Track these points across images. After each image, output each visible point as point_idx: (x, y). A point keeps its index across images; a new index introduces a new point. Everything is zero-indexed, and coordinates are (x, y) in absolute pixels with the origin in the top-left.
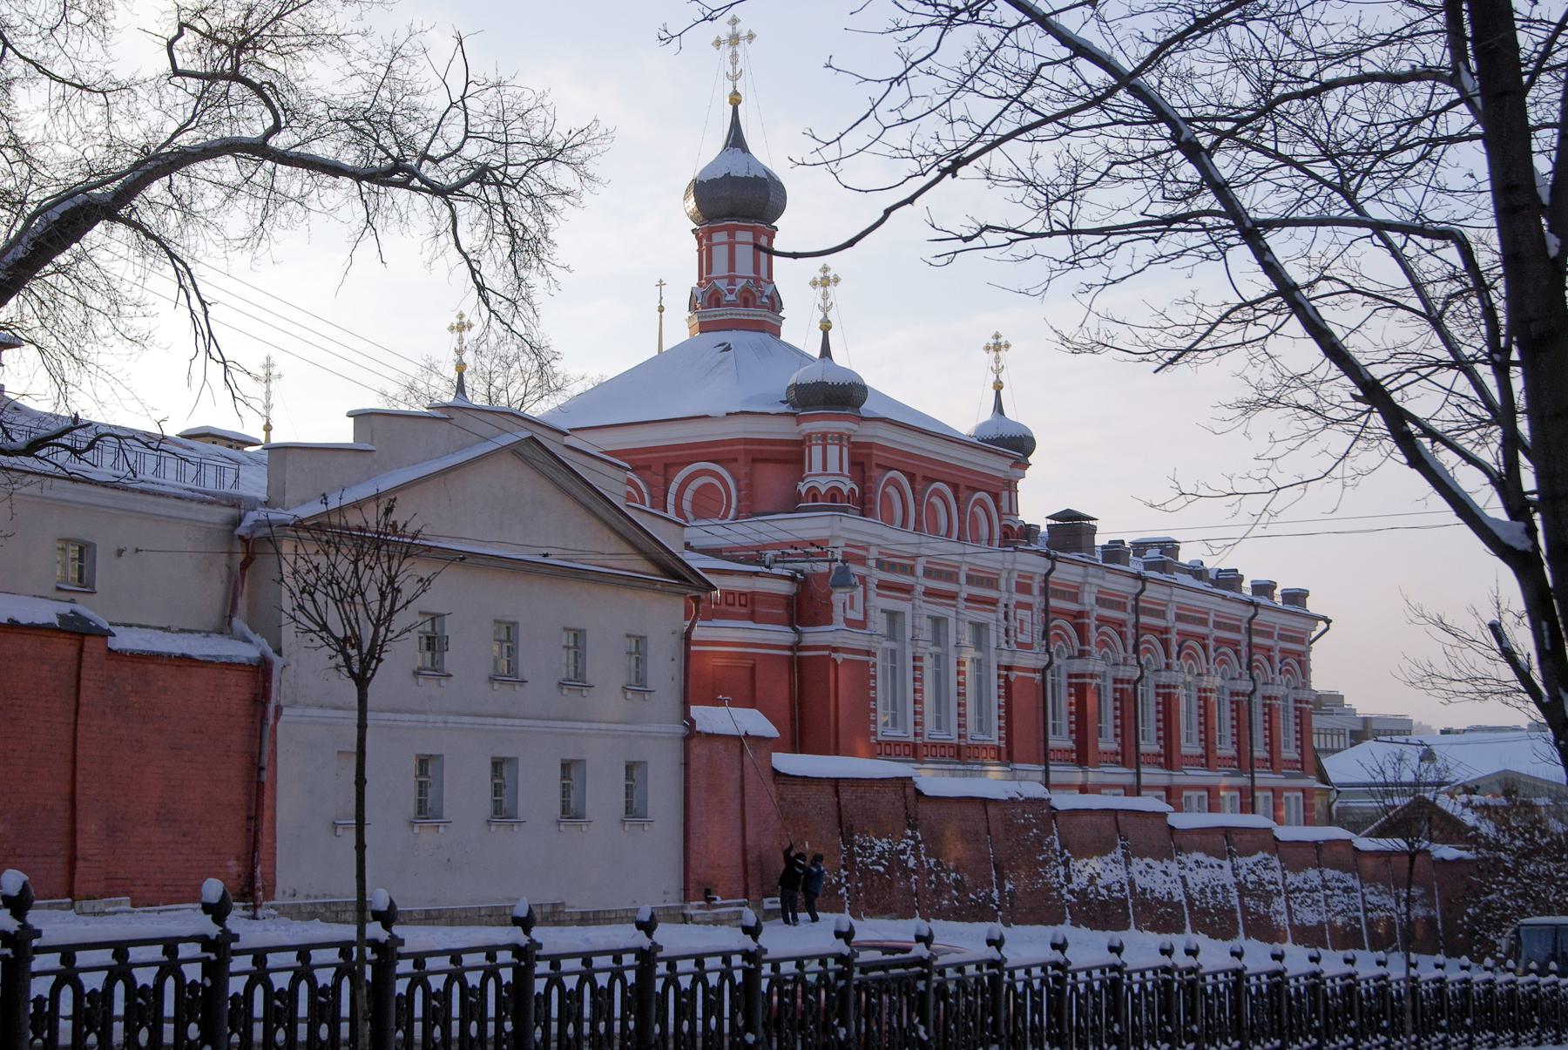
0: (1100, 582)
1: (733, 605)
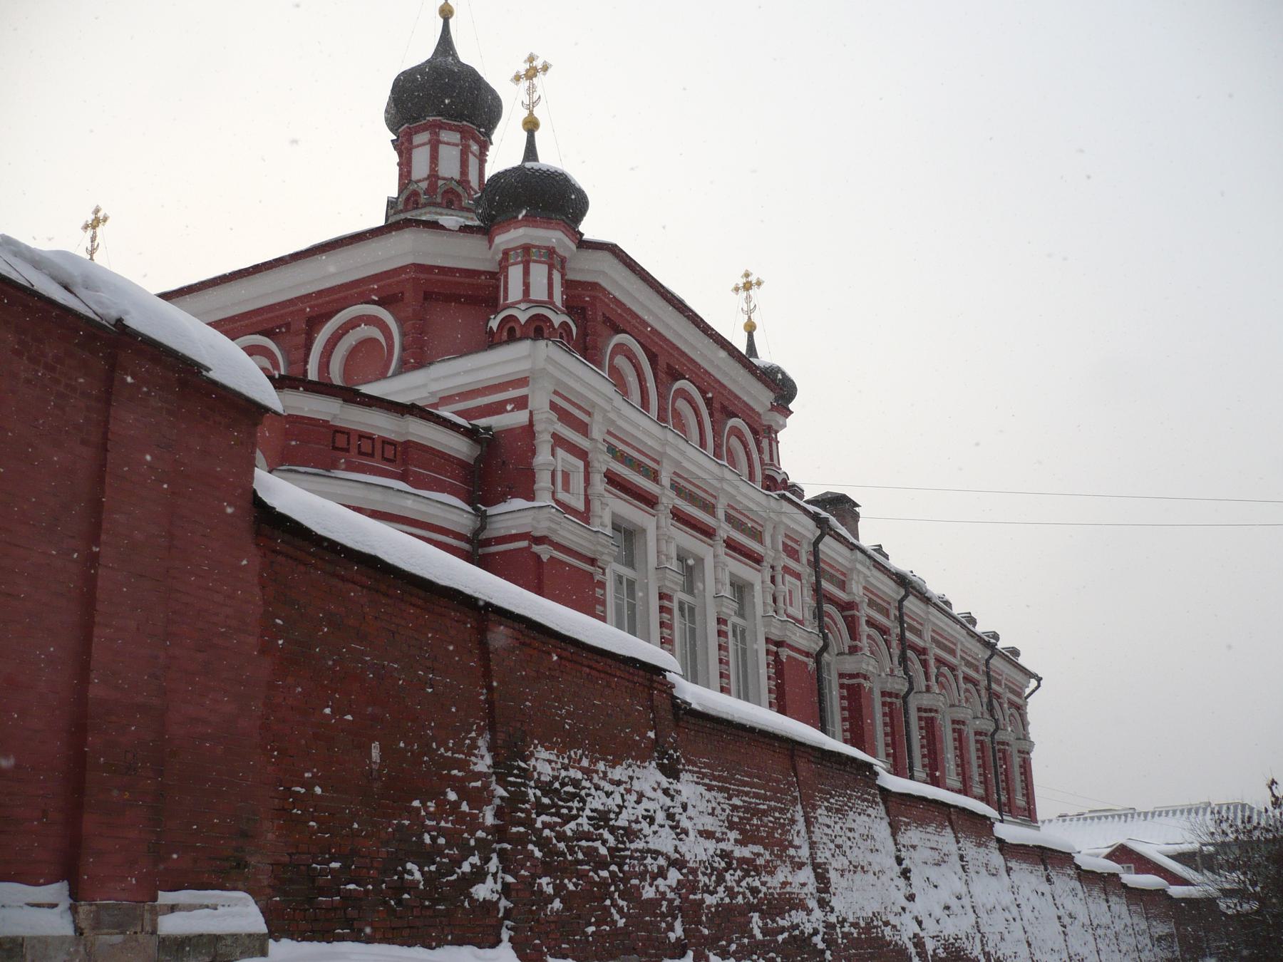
1: (372, 455)
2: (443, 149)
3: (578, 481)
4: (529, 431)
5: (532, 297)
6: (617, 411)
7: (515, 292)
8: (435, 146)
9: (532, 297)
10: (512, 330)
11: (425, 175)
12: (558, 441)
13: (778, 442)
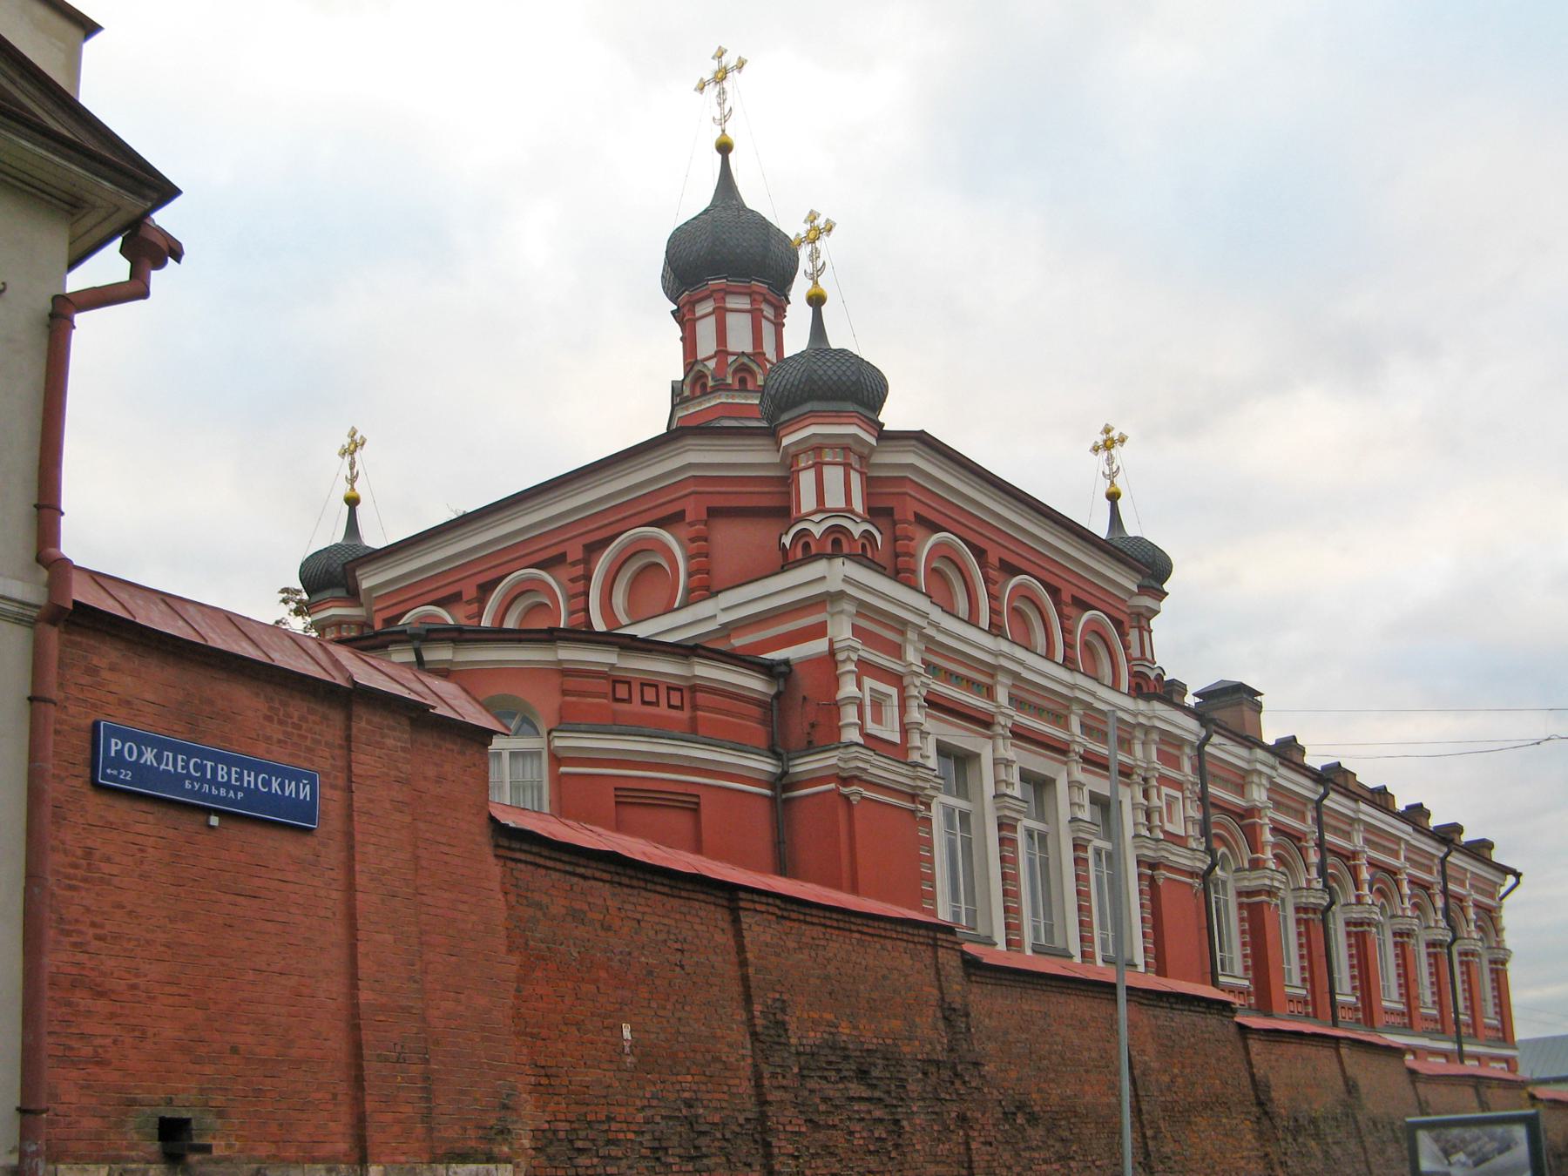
0: (1274, 774)
1: (656, 704)
2: (731, 319)
3: (892, 712)
4: (831, 658)
5: (828, 505)
6: (937, 626)
7: (808, 502)
8: (720, 313)
9: (828, 505)
10: (806, 546)
11: (712, 352)
12: (865, 667)
13: (1150, 632)
